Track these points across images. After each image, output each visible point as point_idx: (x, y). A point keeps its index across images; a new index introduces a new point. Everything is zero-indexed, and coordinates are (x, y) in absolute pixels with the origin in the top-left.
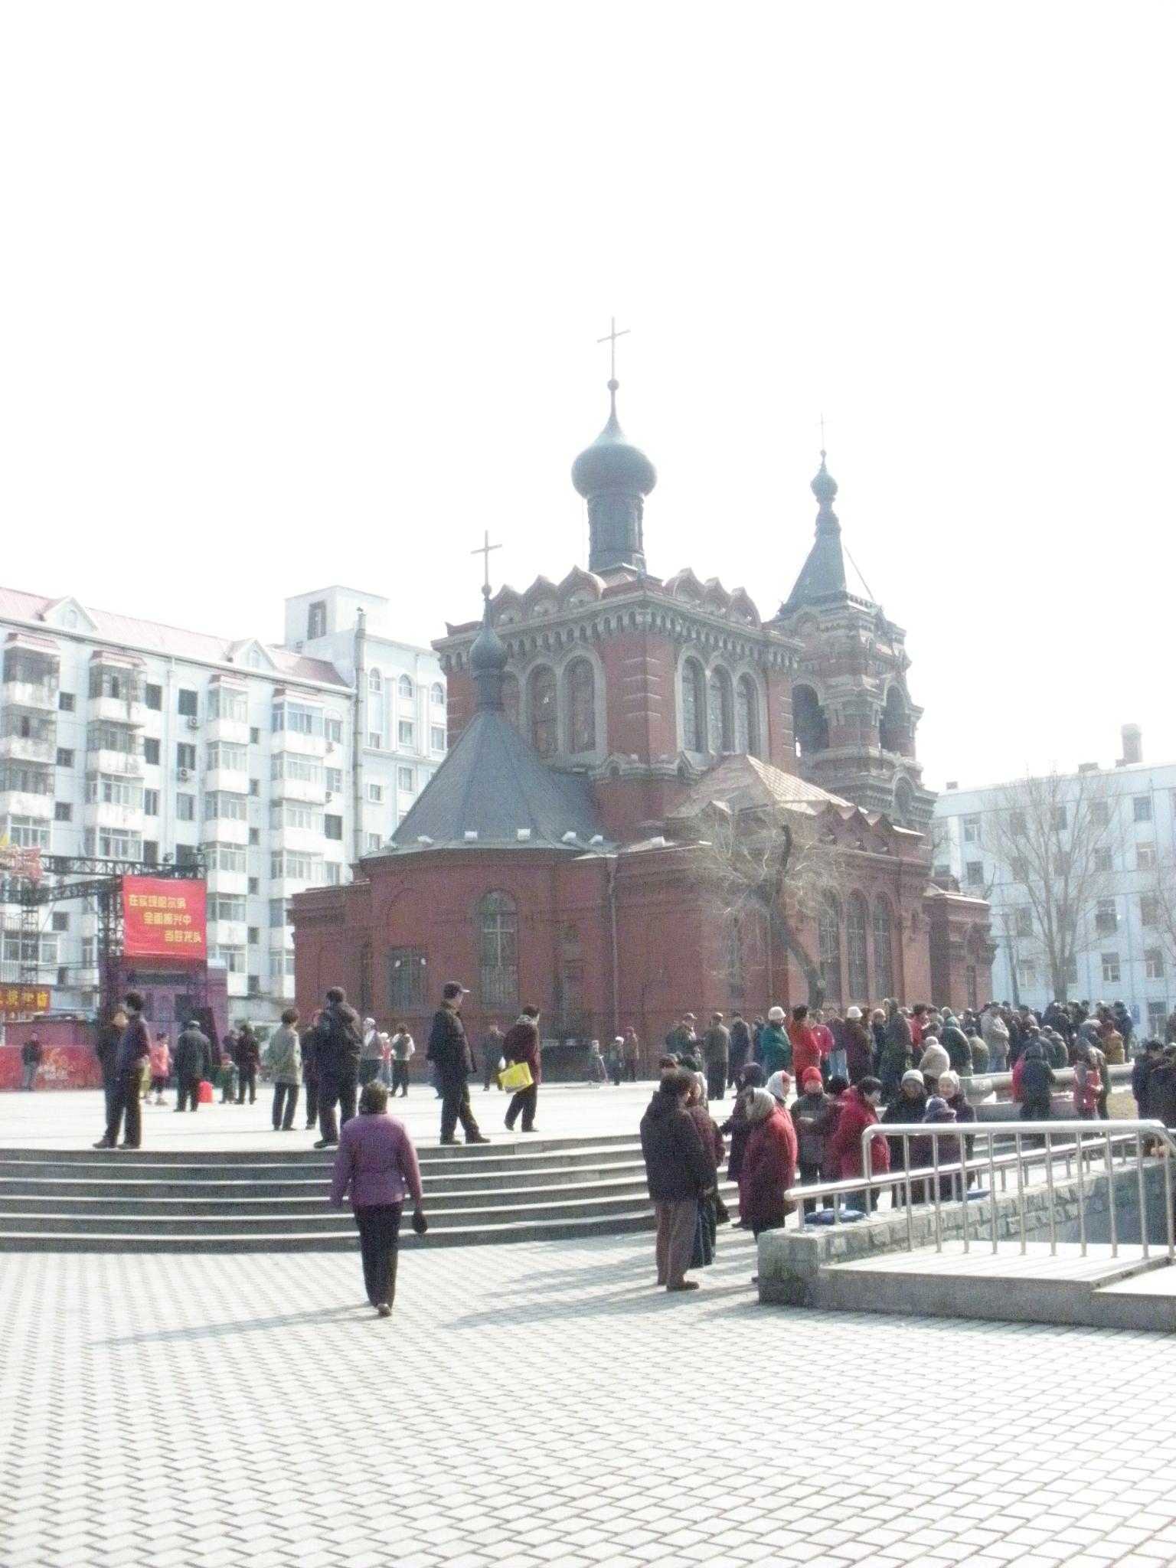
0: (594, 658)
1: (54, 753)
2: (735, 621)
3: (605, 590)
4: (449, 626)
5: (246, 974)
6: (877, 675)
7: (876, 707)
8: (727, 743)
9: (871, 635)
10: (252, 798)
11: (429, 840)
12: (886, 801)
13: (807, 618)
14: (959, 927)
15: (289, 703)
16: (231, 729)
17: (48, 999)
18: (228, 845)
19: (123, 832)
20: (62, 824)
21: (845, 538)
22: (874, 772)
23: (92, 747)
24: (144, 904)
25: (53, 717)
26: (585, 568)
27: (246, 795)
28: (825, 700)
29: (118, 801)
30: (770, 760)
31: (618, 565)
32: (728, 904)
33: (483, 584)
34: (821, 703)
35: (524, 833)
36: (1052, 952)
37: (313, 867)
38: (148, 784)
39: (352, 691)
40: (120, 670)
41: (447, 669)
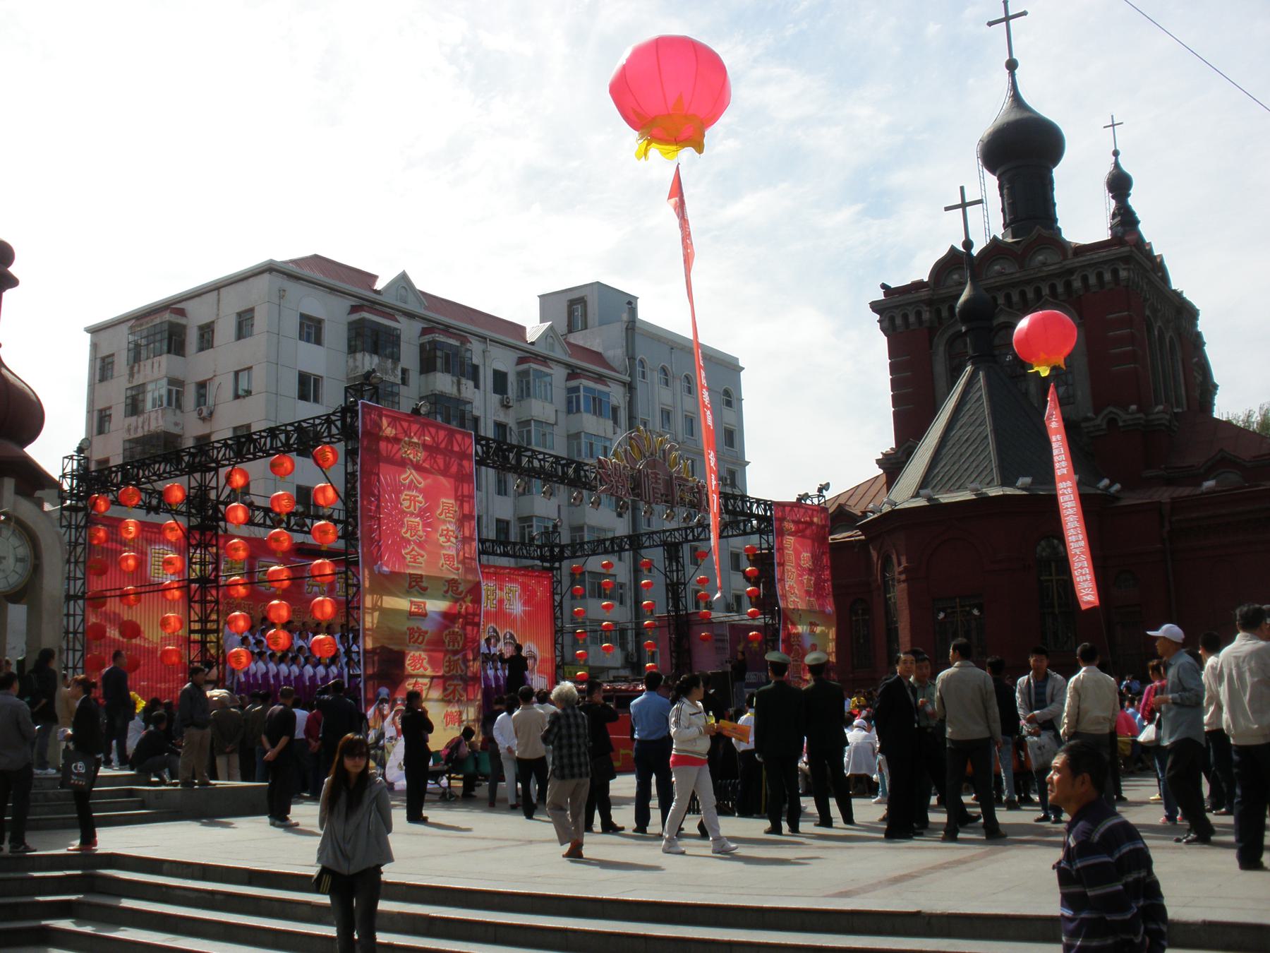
25: (395, 389)
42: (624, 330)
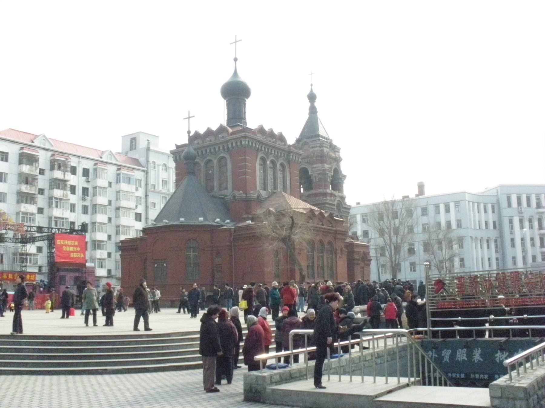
0: (227, 156)
1: (37, 189)
2: (278, 144)
3: (231, 132)
4: (176, 145)
5: (107, 269)
6: (330, 164)
7: (329, 175)
8: (275, 187)
9: (328, 150)
10: (109, 207)
11: (167, 221)
12: (333, 208)
13: (306, 143)
14: (358, 253)
15: (123, 174)
16: (101, 182)
17: (35, 277)
18: (100, 223)
19: (63, 218)
20: (40, 215)
21: (319, 115)
22: (328, 198)
23: (51, 188)
24: (62, 243)
25: (37, 177)
26: (225, 124)
27: (107, 206)
28: (311, 172)
29: (61, 207)
30: (291, 194)
31: (236, 124)
32: (270, 244)
33: (188, 130)
34: (310, 174)
35: (201, 219)
36: (392, 262)
37: (131, 231)
38: (71, 201)
39: (145, 169)
40: (62, 161)
41: (175, 161)
42: (146, 151)
